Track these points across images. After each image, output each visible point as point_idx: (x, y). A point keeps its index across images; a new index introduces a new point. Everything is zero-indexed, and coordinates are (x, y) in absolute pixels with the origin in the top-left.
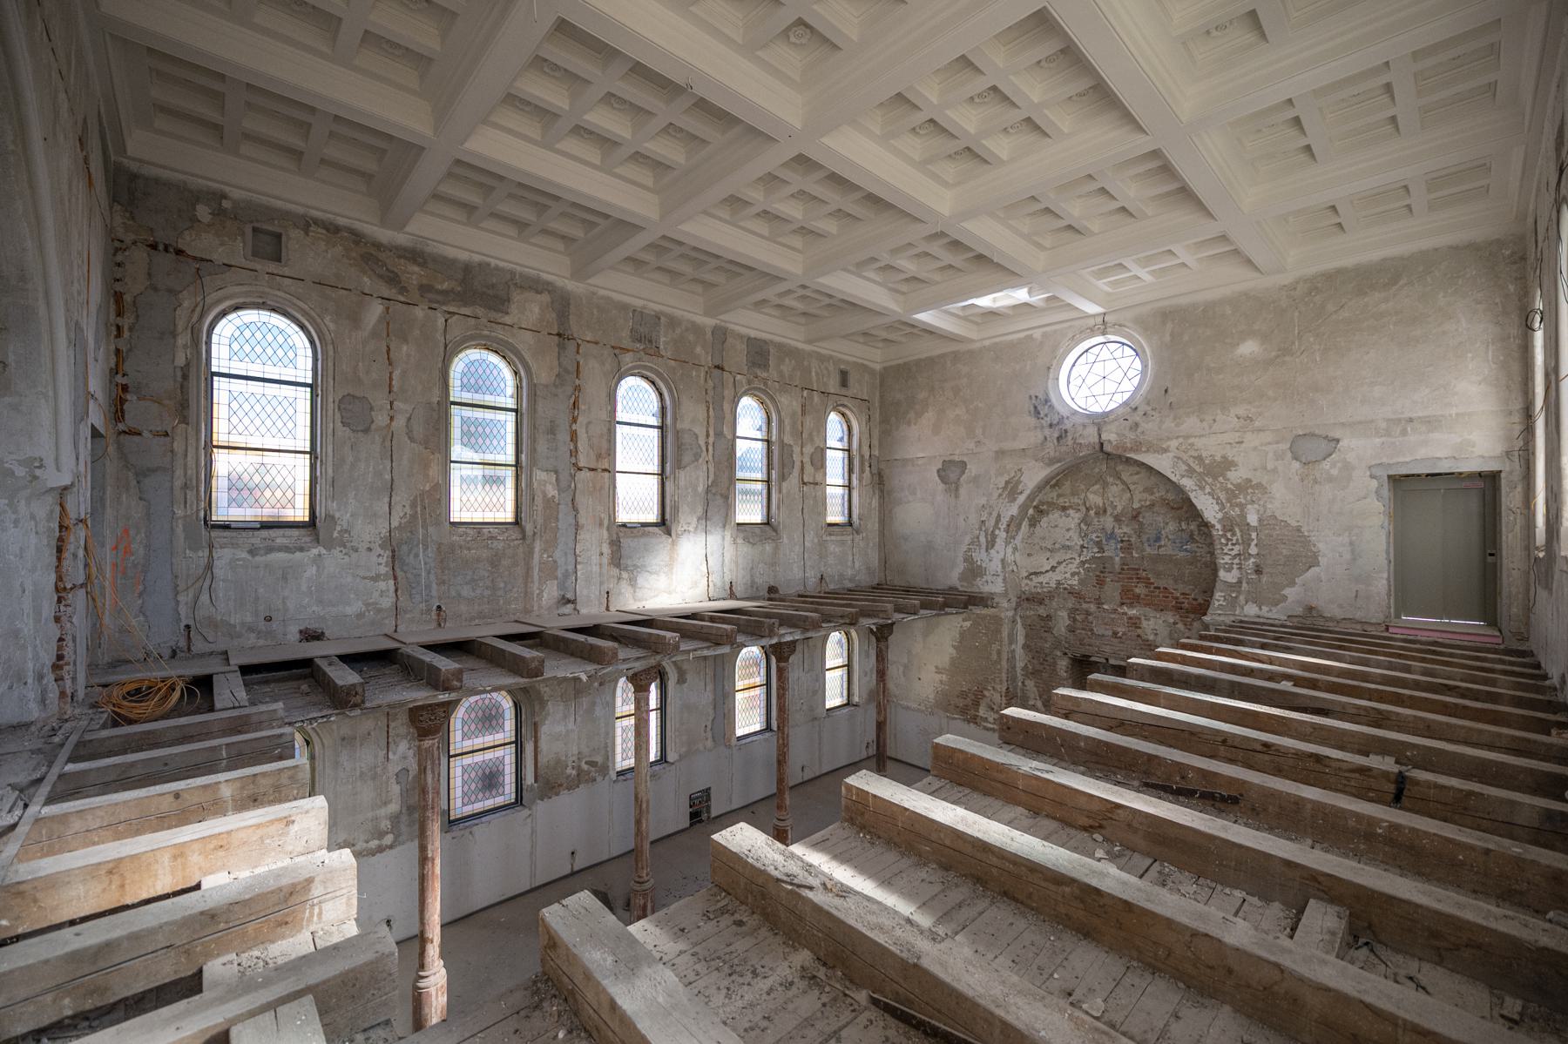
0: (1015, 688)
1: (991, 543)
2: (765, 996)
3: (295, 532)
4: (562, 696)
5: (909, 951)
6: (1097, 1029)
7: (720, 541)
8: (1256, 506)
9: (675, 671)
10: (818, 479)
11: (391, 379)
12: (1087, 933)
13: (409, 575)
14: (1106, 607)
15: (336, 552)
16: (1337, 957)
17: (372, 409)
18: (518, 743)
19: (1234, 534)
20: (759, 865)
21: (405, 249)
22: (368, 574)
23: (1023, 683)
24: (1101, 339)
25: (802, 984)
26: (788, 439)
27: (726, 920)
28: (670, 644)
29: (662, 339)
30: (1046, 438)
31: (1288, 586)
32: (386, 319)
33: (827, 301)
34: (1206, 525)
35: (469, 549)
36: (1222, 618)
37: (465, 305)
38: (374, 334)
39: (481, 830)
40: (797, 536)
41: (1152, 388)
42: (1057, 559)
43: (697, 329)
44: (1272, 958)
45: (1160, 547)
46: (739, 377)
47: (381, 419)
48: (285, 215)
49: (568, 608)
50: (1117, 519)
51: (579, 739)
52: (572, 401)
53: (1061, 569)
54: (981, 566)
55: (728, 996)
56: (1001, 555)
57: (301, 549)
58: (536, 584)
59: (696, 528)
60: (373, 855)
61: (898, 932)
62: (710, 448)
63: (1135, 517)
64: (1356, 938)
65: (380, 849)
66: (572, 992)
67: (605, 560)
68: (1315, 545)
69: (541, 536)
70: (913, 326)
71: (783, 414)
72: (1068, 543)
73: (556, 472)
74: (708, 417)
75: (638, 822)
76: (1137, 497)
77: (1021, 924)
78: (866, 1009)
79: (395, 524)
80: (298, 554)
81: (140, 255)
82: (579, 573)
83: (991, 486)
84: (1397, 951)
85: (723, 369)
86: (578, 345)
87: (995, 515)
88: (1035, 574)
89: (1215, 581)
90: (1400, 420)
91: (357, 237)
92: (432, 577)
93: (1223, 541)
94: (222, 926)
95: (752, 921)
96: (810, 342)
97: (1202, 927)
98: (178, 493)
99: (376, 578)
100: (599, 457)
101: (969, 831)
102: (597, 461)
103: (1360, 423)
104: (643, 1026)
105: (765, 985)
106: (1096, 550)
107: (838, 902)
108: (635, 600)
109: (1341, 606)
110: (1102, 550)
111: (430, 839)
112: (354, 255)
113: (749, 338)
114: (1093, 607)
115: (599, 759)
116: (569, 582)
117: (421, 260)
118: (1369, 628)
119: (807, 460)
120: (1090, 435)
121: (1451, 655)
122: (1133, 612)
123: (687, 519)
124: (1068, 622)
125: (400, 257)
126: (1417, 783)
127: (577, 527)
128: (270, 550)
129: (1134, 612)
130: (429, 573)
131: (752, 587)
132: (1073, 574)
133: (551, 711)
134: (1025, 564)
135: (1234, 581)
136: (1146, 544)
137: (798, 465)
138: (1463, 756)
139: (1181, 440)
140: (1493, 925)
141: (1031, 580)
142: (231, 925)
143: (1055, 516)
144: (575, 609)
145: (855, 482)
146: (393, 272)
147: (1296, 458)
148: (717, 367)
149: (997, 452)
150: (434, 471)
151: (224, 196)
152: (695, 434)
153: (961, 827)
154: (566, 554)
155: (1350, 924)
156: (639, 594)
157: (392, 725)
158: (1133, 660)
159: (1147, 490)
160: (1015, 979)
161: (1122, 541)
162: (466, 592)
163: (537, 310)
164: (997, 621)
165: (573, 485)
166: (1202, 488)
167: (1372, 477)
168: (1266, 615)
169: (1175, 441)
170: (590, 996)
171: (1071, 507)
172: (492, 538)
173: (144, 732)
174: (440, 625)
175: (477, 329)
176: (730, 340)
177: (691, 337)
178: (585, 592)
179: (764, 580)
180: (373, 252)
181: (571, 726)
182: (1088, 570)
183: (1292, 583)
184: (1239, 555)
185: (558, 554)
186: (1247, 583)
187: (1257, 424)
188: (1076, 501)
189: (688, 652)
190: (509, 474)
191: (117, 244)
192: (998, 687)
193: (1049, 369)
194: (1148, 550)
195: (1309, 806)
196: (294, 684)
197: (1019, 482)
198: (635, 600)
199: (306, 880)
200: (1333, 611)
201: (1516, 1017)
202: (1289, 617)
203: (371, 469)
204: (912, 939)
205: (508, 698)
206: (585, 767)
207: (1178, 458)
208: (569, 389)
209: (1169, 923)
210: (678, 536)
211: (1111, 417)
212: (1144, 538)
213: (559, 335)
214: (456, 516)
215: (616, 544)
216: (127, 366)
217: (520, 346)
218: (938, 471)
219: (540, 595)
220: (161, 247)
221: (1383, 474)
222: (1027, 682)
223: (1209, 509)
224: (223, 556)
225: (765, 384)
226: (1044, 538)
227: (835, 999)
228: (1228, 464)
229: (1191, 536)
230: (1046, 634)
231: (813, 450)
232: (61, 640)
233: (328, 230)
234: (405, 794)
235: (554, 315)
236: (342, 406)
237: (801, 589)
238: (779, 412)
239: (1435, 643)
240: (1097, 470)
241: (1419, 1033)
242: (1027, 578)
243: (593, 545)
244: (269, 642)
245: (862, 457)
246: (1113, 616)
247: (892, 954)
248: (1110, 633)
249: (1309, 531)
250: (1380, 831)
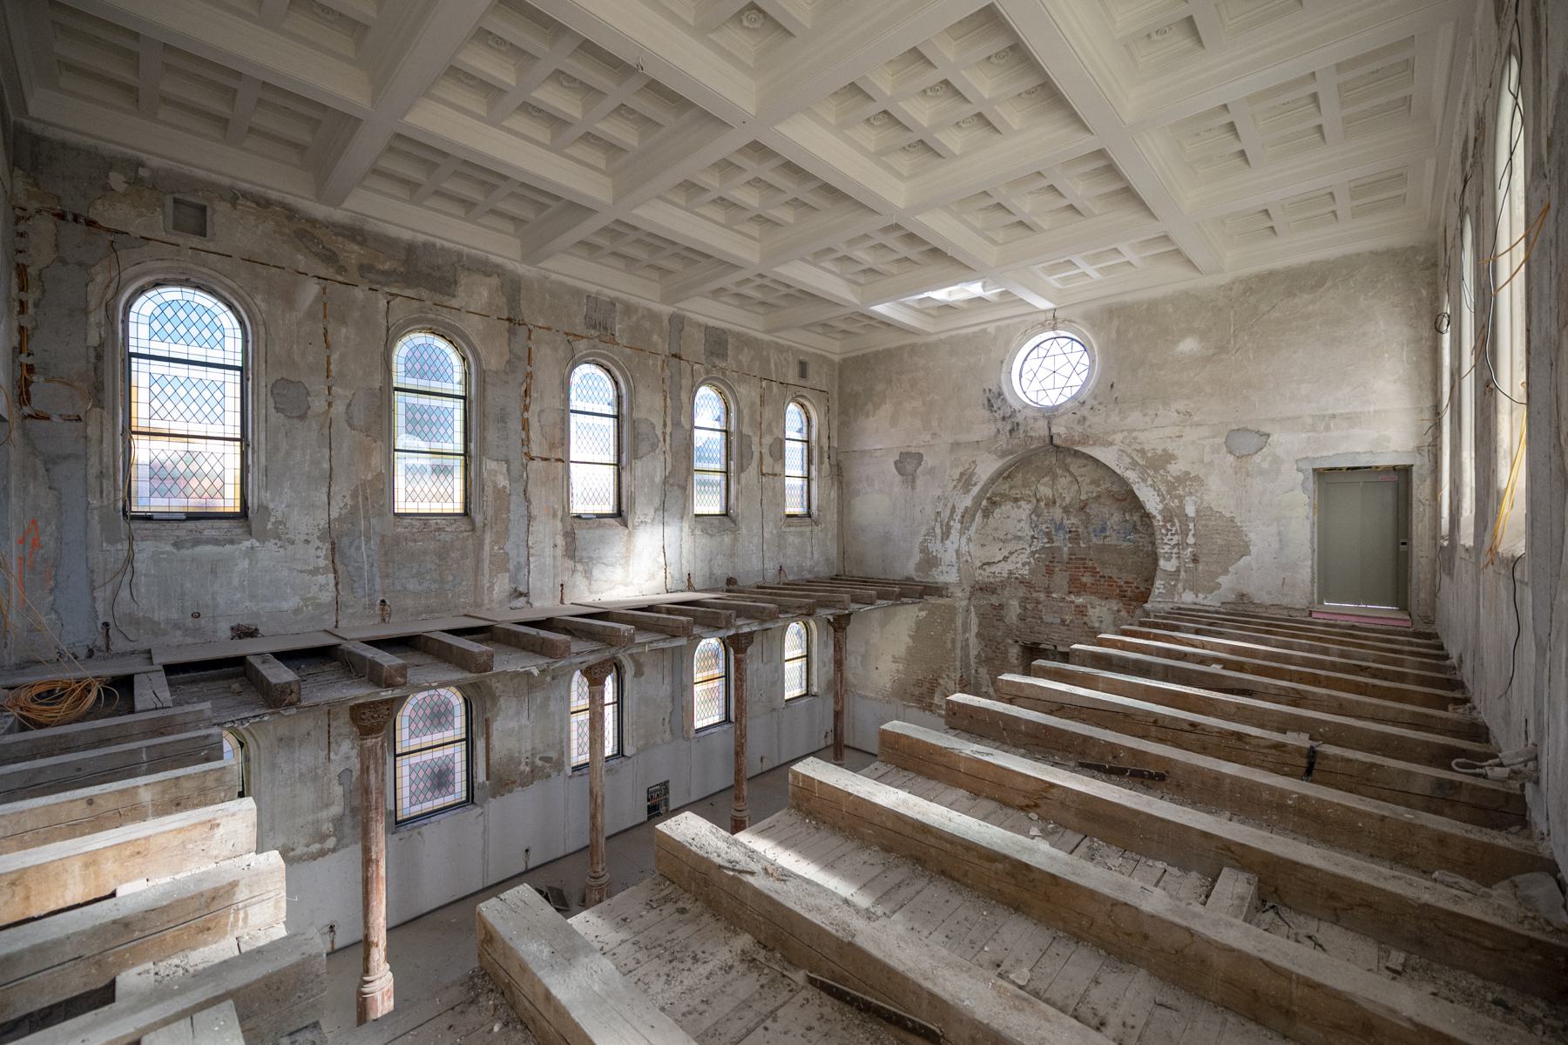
0: (969, 675)
1: (946, 534)
2: (704, 981)
3: (225, 524)
4: (514, 692)
5: (844, 930)
6: (1017, 997)
7: (678, 533)
8: (1194, 498)
9: (632, 665)
10: (777, 470)
11: (329, 363)
12: (1017, 907)
13: (350, 568)
14: (1054, 595)
15: (270, 544)
16: (1245, 920)
17: (308, 394)
18: (469, 740)
19: (1173, 525)
20: (701, 853)
21: (343, 227)
22: (306, 567)
23: (976, 671)
24: (1051, 334)
25: (741, 968)
26: (746, 430)
27: (669, 908)
28: (624, 637)
29: (617, 327)
30: (999, 431)
31: (1222, 574)
32: (323, 299)
33: (784, 290)
34: (1147, 516)
35: (415, 541)
36: (1161, 606)
37: (409, 286)
38: (310, 315)
39: (430, 830)
40: (756, 527)
41: (1099, 382)
42: (1009, 550)
43: (653, 316)
44: (1185, 924)
45: (1105, 537)
46: (696, 367)
47: (318, 404)
48: (210, 187)
49: (521, 601)
50: (1066, 510)
51: (533, 735)
52: (523, 389)
53: (1013, 558)
54: (936, 557)
55: (668, 982)
56: (956, 546)
57: (232, 542)
59: (653, 520)
60: (315, 859)
61: (835, 913)
62: (668, 438)
63: (1082, 509)
64: (1264, 902)
65: (322, 853)
66: (509, 985)
67: (559, 552)
68: (1246, 535)
69: (492, 528)
70: (871, 318)
71: (741, 404)
72: (1019, 534)
73: (507, 462)
74: (665, 407)
75: (593, 817)
76: (1085, 488)
77: (956, 900)
78: (803, 988)
79: (334, 514)
80: (228, 547)
81: (44, 227)
82: (531, 567)
83: (947, 477)
84: (1300, 913)
85: (680, 358)
87: (950, 505)
88: (988, 564)
89: (1155, 570)
90: (1324, 416)
91: (290, 212)
92: (375, 570)
93: (1163, 531)
94: (137, 934)
95: (694, 908)
96: (769, 332)
97: (1122, 897)
98: (92, 481)
99: (315, 572)
100: (552, 446)
101: (909, 814)
103: (1288, 418)
104: (577, 1014)
105: (703, 970)
106: (1046, 540)
107: (778, 885)
108: (591, 593)
109: (1269, 593)
110: (1051, 540)
111: (374, 840)
112: (287, 231)
113: (707, 327)
114: (1042, 596)
115: (554, 755)
116: (522, 574)
117: (359, 238)
118: (1293, 613)
119: (765, 451)
120: (1040, 429)
121: (1366, 638)
122: (1080, 600)
123: (643, 511)
124: (1019, 611)
125: (336, 234)
126: (1326, 757)
127: (530, 518)
129: (1081, 600)
130: (372, 565)
131: (710, 578)
132: (1024, 564)
133: (504, 706)
134: (979, 555)
135: (1173, 570)
136: (1092, 535)
137: (756, 456)
138: (1369, 731)
139: (1125, 433)
140: (1382, 884)
141: (985, 570)
142: (147, 933)
143: (1007, 507)
144: (528, 602)
145: (814, 473)
146: (330, 250)
147: (1231, 453)
148: (674, 356)
149: (952, 444)
150: (376, 460)
151: (141, 164)
153: (902, 810)
154: (518, 546)
155: (1259, 889)
156: (595, 586)
157: (334, 724)
158: (1076, 646)
159: (1095, 482)
160: (945, 952)
161: (1070, 532)
162: (412, 585)
163: (485, 294)
164: (952, 609)
165: (525, 475)
166: (1144, 480)
167: (1299, 470)
168: (1202, 602)
169: (1119, 434)
170: (526, 989)
171: (1022, 498)
172: (439, 530)
173: (54, 736)
174: (384, 620)
175: (421, 312)
176: (687, 328)
177: (647, 325)
178: (538, 584)
179: (722, 570)
180: (309, 229)
181: (524, 721)
182: (1038, 560)
183: (1226, 572)
184: (1178, 544)
185: (509, 546)
186: (1185, 572)
187: (1195, 418)
188: (1028, 492)
189: (643, 644)
190: (458, 463)
191: (19, 212)
192: (952, 675)
193: (1003, 363)
194: (1094, 540)
195: (1228, 781)
196: (225, 683)
197: (972, 474)
198: (591, 593)
199: (230, 884)
200: (1263, 598)
201: (1399, 968)
202: (1223, 603)
203: (308, 457)
204: (848, 919)
205: (458, 694)
206: (539, 763)
207: (1123, 451)
208: (520, 377)
209: (1092, 894)
210: (634, 527)
211: (1061, 411)
212: (1091, 529)
213: (509, 320)
214: (402, 505)
215: (570, 536)
216: (33, 345)
217: (468, 332)
218: (895, 463)
219: (491, 588)
220: (70, 217)
221: (1309, 467)
222: (980, 670)
223: (1151, 500)
224: (145, 551)
225: (724, 374)
226: (996, 529)
227: (773, 980)
228: (1168, 458)
229: (1135, 526)
230: (996, 623)
231: (771, 441)
233: (258, 204)
234: (348, 795)
235: (504, 300)
236: (275, 391)
237: (759, 580)
238: (737, 403)
239: (1353, 627)
240: (1047, 463)
241: (1310, 986)
242: (980, 568)
244: (198, 641)
245: (821, 448)
246: (1061, 604)
247: (829, 934)
248: (1059, 621)
249: (1241, 522)
250: (1290, 802)
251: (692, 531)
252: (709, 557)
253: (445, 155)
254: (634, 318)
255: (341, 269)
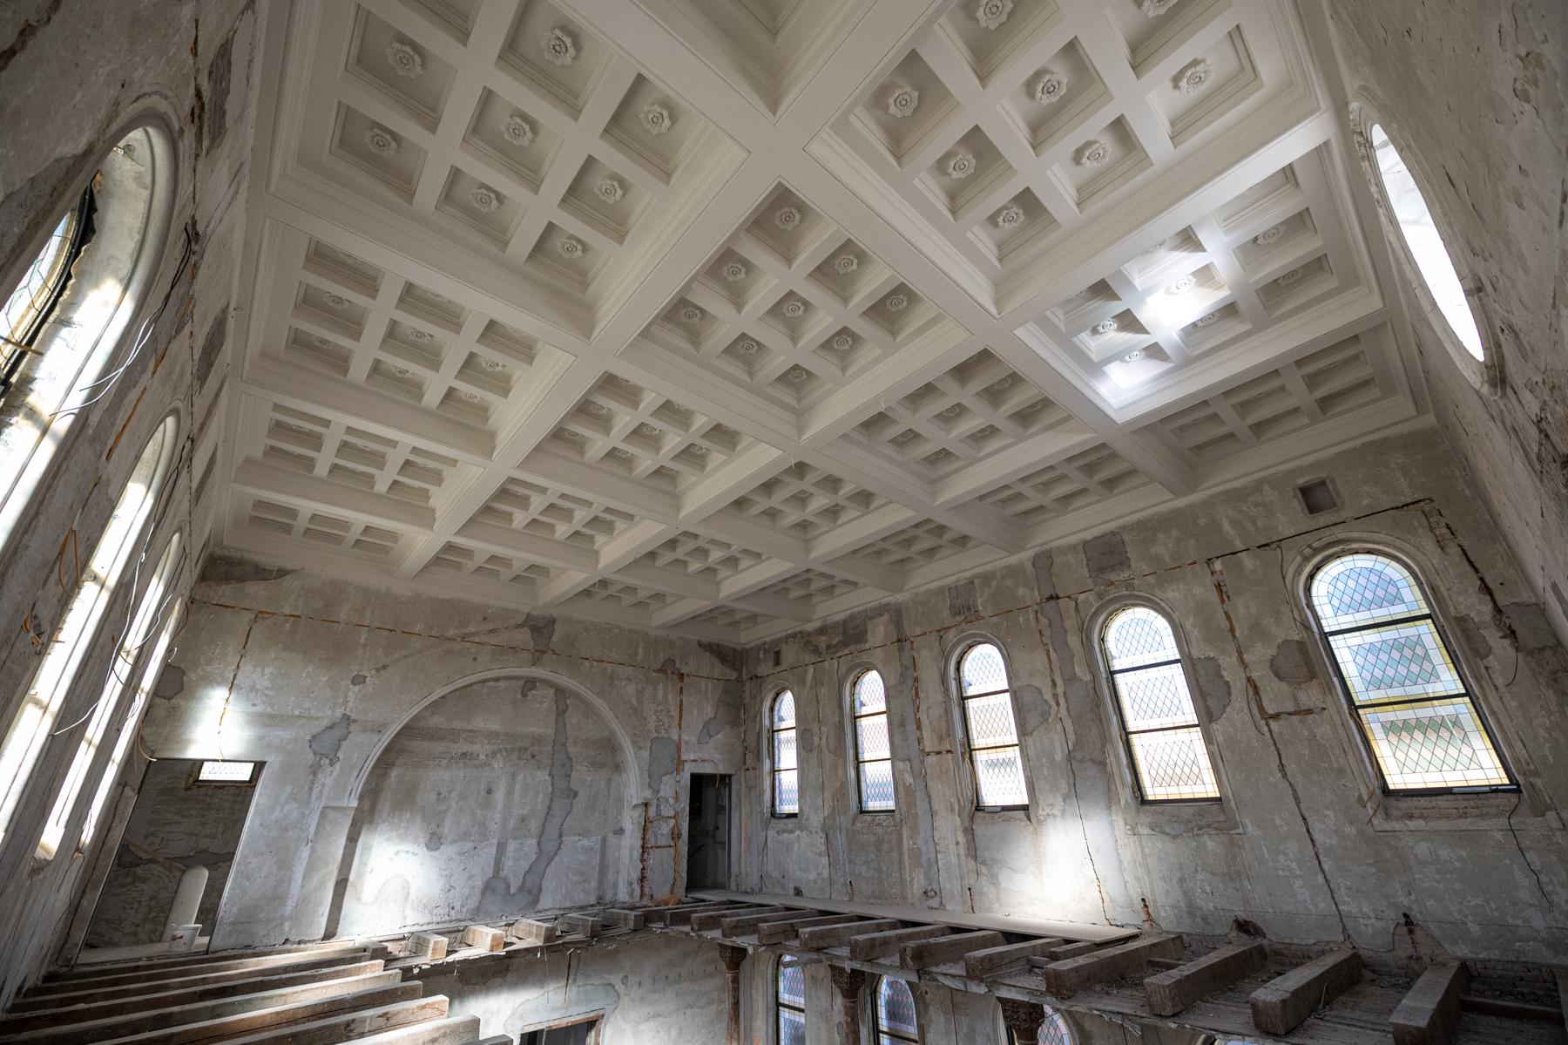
37: (846, 647)
38: (811, 686)
43: (1014, 571)
46: (1082, 597)
47: (816, 740)
48: (778, 642)
52: (914, 692)
58: (908, 871)
62: (1062, 701)
67: (962, 851)
73: (910, 761)
74: (1050, 661)
79: (826, 814)
82: (940, 863)
85: (1058, 598)
86: (912, 642)
91: (801, 633)
99: (820, 855)
100: (941, 739)
102: (940, 744)
119: (1260, 673)
127: (932, 814)
128: (783, 832)
133: (934, 1018)
148: (1051, 598)
152: (1037, 688)
163: (882, 629)
177: (1009, 583)
178: (948, 886)
208: (910, 683)
225: (1129, 586)
231: (1272, 651)
232: (643, 869)
235: (893, 627)
243: (948, 829)
251: (1133, 829)
252: (1178, 875)
253: (1355, 338)
254: (994, 584)
255: (820, 653)
